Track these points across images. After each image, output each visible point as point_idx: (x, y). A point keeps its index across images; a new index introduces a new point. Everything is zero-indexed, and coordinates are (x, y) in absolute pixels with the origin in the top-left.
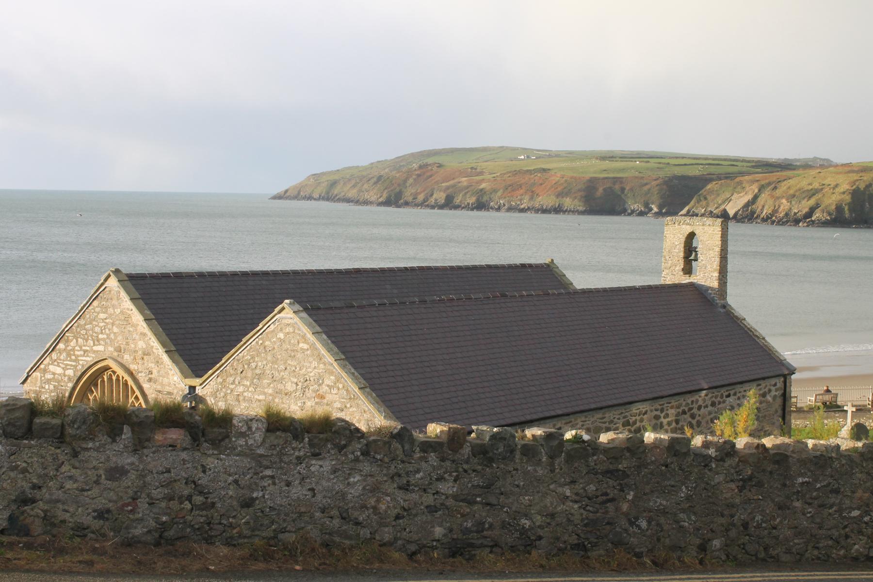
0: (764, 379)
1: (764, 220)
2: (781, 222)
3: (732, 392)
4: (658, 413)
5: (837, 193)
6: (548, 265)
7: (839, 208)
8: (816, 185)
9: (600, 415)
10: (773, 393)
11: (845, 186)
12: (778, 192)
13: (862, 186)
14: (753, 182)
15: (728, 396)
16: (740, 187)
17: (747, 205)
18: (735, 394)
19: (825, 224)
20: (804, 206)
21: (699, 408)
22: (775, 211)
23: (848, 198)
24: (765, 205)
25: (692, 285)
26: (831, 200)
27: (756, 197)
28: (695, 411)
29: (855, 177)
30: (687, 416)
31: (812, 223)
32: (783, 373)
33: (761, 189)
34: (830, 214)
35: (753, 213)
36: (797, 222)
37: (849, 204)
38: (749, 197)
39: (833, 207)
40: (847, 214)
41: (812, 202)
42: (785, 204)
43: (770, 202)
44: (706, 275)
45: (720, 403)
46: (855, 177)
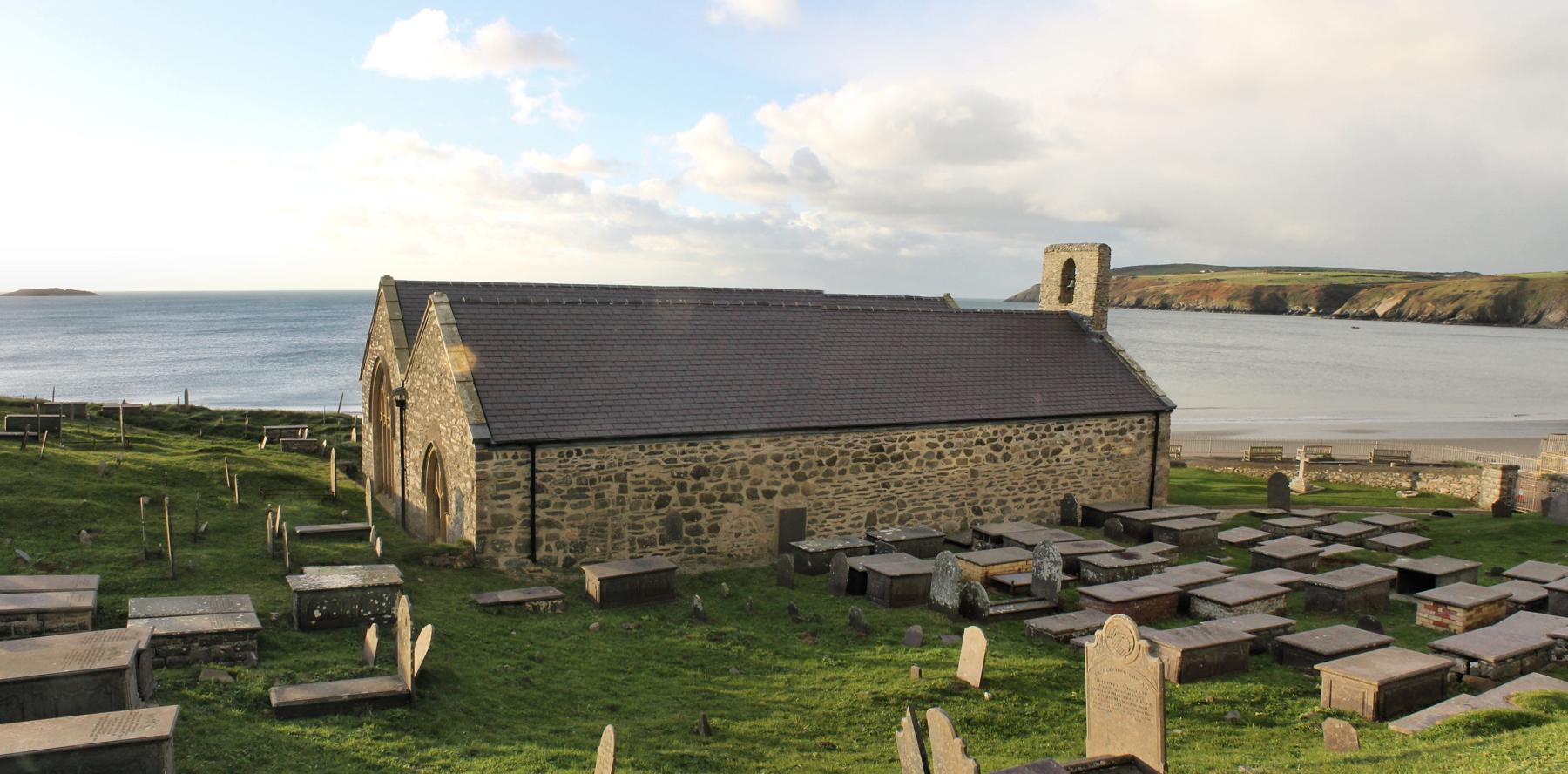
0: (1118, 414)
1: (1411, 319)
2: (1426, 321)
3: (1066, 426)
4: (935, 441)
6: (943, 300)
7: (1482, 310)
8: (1460, 291)
9: (831, 437)
10: (1138, 430)
11: (1488, 293)
12: (1424, 297)
13: (1505, 293)
15: (1061, 429)
16: (1389, 293)
18: (1071, 428)
20: (1449, 308)
21: (1008, 439)
22: (1420, 312)
24: (1412, 307)
25: (1066, 313)
26: (1475, 304)
27: (1404, 301)
28: (1000, 442)
29: (1497, 285)
30: (988, 449)
31: (1455, 322)
32: (1161, 410)
33: (1409, 294)
35: (1400, 313)
36: (1440, 321)
38: (1398, 301)
41: (1457, 304)
42: (1430, 307)
43: (1417, 305)
44: (1083, 304)
45: (1043, 436)
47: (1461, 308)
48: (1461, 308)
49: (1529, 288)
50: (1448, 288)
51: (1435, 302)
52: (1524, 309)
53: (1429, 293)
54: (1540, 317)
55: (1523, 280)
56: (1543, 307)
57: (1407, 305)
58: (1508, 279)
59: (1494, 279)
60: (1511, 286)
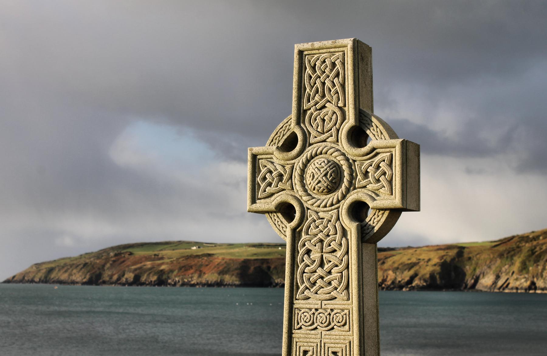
2: (389, 288)
8: (414, 260)
11: (436, 260)
12: (386, 266)
13: (448, 260)
19: (421, 288)
20: (406, 275)
22: (384, 280)
23: (438, 269)
26: (426, 270)
29: (442, 253)
31: (413, 288)
34: (425, 281)
36: (401, 287)
37: (439, 273)
39: (428, 276)
40: (438, 282)
41: (412, 272)
42: (391, 275)
46: (442, 253)
48: (416, 275)
49: (466, 255)
50: (405, 259)
52: (464, 275)
53: (389, 262)
54: (477, 280)
55: (461, 250)
56: (478, 272)
58: (449, 247)
59: (439, 248)
60: (453, 253)
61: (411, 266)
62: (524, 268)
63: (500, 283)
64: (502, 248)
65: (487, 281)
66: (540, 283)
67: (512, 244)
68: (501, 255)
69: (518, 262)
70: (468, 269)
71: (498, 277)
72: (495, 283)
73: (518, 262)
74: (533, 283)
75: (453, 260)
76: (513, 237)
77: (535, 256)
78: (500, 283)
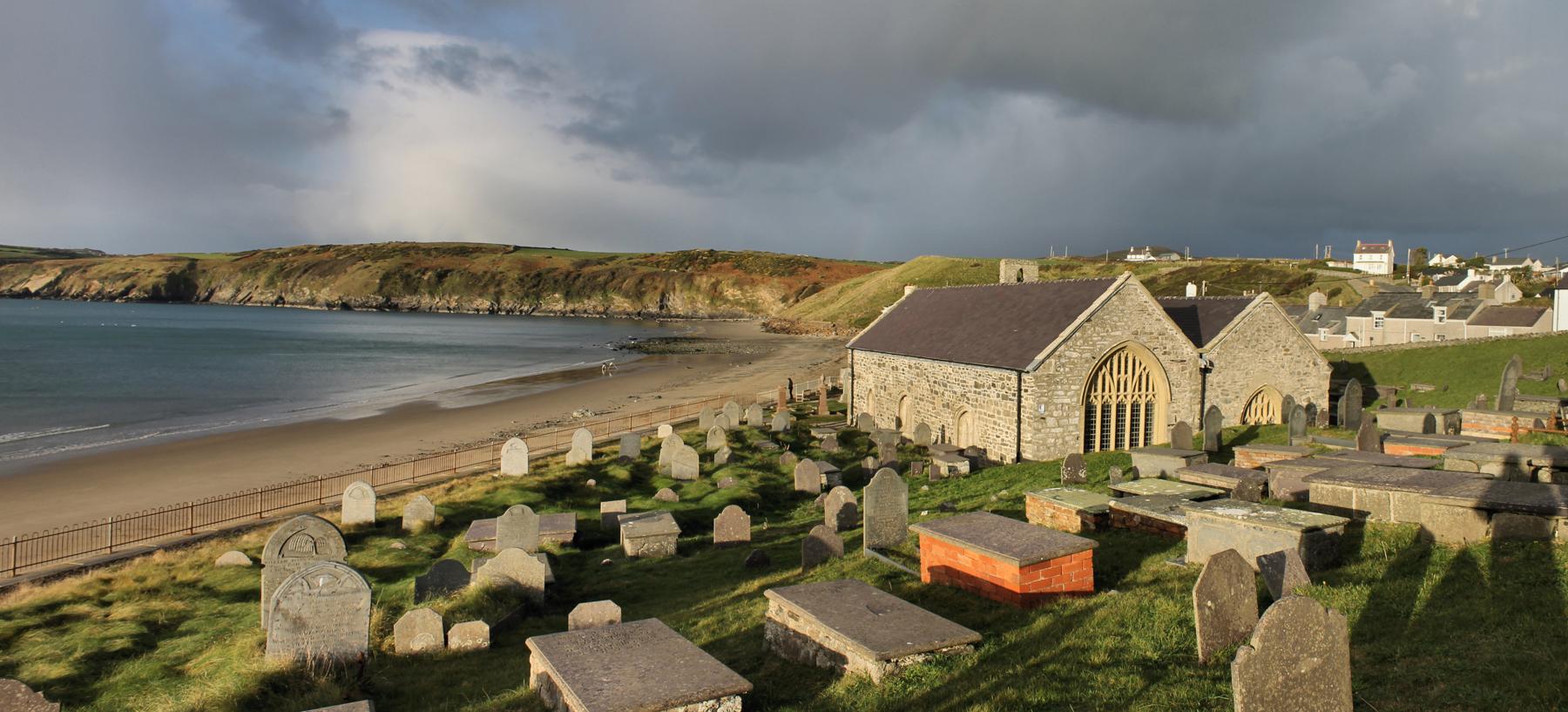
5: (155, 275)
7: (156, 288)
8: (130, 270)
11: (161, 271)
12: (88, 275)
13: (177, 272)
14: (55, 266)
16: (41, 270)
17: (50, 285)
19: (143, 300)
20: (120, 286)
22: (85, 290)
23: (164, 280)
24: (73, 284)
26: (149, 282)
27: (58, 280)
29: (169, 264)
35: (60, 291)
36: (112, 298)
41: (128, 283)
46: (169, 264)
47: (134, 286)
48: (134, 286)
49: (199, 268)
50: (106, 268)
51: (103, 280)
52: (196, 287)
53: (94, 270)
54: (211, 293)
55: (193, 263)
56: (213, 285)
57: (62, 284)
59: (163, 259)
60: (183, 265)
61: (126, 276)
62: (271, 283)
63: (240, 297)
64: (244, 263)
65: (225, 294)
66: (289, 298)
67: (257, 259)
68: (243, 270)
69: (263, 278)
70: (202, 282)
71: (238, 291)
72: (234, 296)
73: (263, 278)
74: (281, 298)
75: (183, 272)
76: (256, 252)
77: (284, 272)
78: (240, 297)
